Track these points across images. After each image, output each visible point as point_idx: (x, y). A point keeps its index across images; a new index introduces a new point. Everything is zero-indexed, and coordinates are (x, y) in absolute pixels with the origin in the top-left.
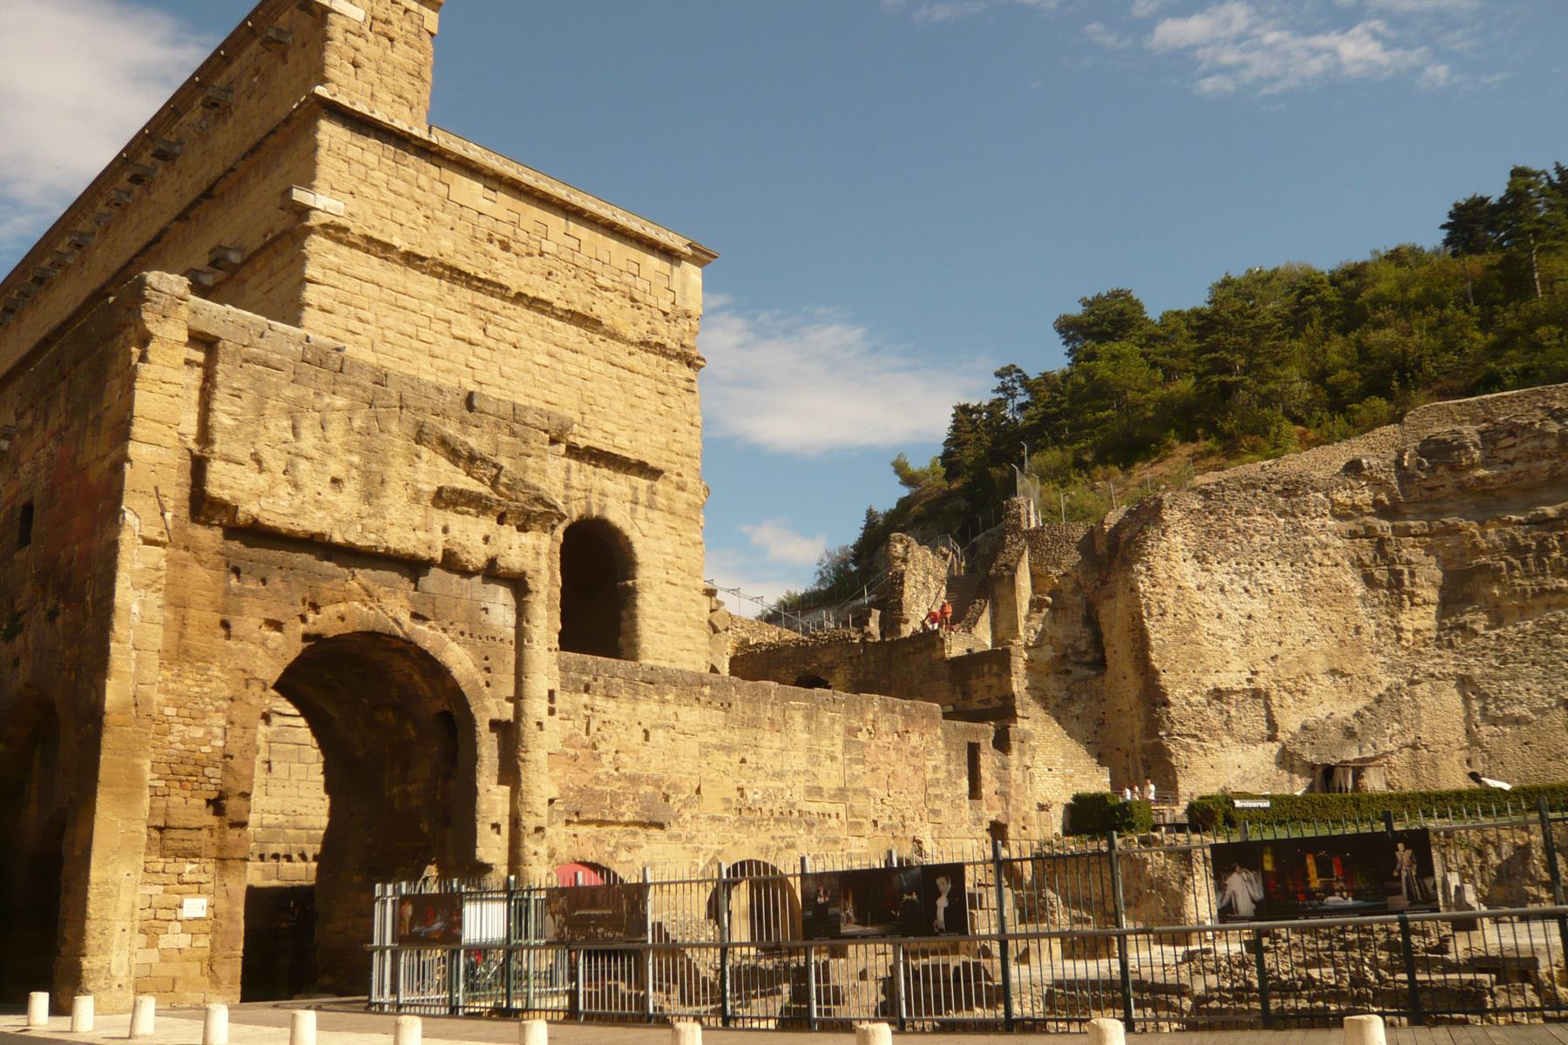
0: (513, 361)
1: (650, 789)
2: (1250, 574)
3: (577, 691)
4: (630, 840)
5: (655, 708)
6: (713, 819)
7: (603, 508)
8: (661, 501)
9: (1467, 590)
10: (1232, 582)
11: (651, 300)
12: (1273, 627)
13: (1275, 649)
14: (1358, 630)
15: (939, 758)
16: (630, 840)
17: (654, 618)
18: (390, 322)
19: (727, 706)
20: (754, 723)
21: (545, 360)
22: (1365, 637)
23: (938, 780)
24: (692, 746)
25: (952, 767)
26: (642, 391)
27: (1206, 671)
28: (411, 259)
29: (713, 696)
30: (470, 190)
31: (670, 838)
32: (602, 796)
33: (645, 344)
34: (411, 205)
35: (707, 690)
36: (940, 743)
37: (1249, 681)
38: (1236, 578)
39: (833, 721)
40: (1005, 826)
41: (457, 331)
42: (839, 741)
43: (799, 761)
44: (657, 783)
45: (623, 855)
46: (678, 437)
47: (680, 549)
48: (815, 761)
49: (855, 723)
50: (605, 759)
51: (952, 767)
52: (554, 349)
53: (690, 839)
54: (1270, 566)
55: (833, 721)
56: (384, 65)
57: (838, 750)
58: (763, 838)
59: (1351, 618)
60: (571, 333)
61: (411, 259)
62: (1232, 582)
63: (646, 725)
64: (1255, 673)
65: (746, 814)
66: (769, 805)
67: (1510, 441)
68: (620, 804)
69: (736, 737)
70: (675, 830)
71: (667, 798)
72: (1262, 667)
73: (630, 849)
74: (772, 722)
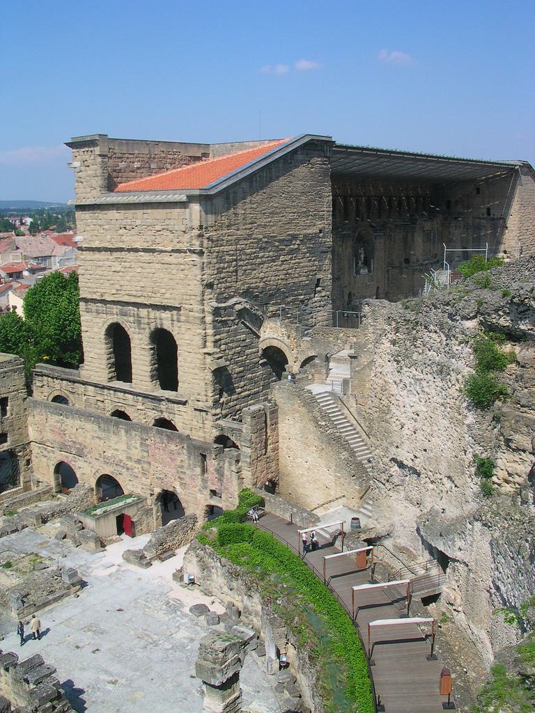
1: (79, 446)
6: (96, 459)
7: (162, 324)
8: (183, 318)
11: (176, 229)
15: (184, 457)
20: (108, 431)
21: (139, 270)
24: (89, 435)
28: (99, 250)
30: (113, 214)
33: (173, 251)
34: (98, 227)
36: (185, 451)
39: (136, 435)
42: (138, 442)
43: (124, 447)
44: (80, 444)
45: (73, 463)
48: (129, 448)
50: (67, 435)
52: (142, 264)
53: (90, 463)
55: (136, 435)
57: (138, 446)
58: (112, 469)
60: (146, 257)
61: (99, 250)
69: (102, 435)
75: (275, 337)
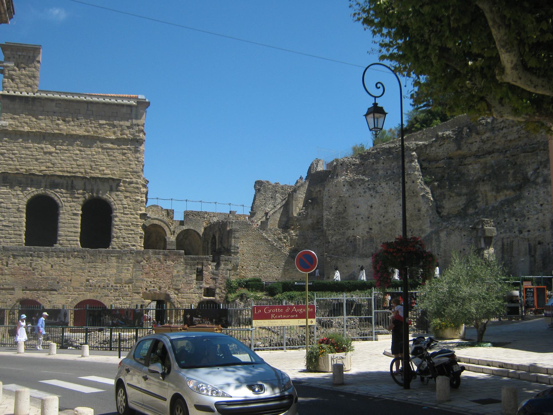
0: (65, 155)
2: (374, 189)
3: (28, 256)
4: (44, 294)
5: (56, 259)
9: (477, 189)
10: (365, 192)
12: (382, 210)
13: (381, 219)
14: (419, 210)
16: (44, 294)
17: (117, 225)
18: (23, 152)
19: (83, 258)
21: (78, 152)
22: (422, 213)
23: (179, 275)
25: (187, 271)
26: (116, 154)
27: (349, 229)
29: (78, 255)
31: (58, 293)
32: (35, 283)
35: (76, 253)
37: (368, 232)
38: (367, 190)
40: (215, 289)
41: (45, 150)
44: (55, 279)
46: (132, 166)
47: (130, 203)
49: (140, 259)
51: (187, 271)
54: (383, 184)
56: (22, 77)
59: (417, 205)
62: (365, 192)
63: (52, 263)
64: (371, 229)
65: (90, 287)
66: (99, 284)
68: (41, 285)
70: (60, 291)
71: (58, 283)
72: (374, 227)
73: (43, 297)
74: (102, 260)
75: (156, 217)
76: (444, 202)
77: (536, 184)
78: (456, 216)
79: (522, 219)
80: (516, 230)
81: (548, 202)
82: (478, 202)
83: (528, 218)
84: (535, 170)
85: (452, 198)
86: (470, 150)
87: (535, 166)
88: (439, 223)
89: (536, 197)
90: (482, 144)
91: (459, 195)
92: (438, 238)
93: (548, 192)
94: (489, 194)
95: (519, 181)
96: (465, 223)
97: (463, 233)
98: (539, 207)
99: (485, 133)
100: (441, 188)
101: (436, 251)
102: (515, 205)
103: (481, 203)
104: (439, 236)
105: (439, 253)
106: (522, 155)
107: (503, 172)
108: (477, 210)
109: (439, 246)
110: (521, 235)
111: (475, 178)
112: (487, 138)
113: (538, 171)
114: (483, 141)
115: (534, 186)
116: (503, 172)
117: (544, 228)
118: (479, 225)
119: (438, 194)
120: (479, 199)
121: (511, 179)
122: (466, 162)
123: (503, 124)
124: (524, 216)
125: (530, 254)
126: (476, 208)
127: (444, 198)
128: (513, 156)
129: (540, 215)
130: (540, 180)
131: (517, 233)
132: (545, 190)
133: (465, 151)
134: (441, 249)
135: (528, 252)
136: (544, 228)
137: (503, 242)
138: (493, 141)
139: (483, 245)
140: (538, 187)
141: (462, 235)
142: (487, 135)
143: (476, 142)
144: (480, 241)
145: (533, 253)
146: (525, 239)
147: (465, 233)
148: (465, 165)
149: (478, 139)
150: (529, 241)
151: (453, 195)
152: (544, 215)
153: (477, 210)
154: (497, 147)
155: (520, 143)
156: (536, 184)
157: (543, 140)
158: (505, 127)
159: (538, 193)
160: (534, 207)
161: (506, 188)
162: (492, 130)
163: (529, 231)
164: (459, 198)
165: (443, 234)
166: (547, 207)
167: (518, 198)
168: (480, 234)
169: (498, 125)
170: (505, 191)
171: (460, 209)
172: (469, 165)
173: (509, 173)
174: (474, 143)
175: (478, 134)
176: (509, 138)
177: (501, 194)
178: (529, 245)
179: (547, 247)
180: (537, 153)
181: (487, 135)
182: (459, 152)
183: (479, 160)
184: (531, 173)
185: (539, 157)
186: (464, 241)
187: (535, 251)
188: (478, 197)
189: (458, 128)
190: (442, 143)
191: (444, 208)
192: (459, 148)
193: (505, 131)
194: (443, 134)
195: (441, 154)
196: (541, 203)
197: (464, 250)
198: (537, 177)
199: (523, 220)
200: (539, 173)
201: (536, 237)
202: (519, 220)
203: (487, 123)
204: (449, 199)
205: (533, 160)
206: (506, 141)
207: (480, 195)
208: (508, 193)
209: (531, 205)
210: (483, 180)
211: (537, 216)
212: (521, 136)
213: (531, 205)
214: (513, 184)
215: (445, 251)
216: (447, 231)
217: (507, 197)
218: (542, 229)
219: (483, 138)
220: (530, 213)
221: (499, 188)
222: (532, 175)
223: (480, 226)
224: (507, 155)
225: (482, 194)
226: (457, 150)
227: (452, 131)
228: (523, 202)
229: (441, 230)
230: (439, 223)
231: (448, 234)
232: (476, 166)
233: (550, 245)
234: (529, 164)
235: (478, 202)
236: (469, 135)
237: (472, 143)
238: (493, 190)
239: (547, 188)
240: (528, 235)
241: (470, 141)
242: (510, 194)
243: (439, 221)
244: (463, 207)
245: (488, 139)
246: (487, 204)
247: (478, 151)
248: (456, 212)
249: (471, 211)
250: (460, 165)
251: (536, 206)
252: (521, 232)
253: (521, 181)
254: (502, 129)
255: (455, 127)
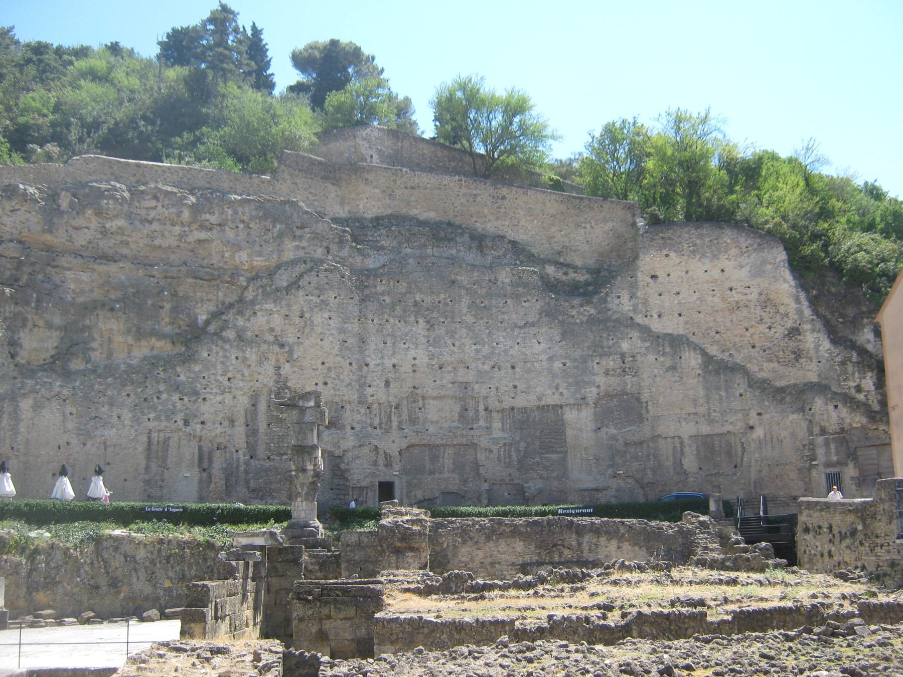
9: (87, 322)
67: (153, 203)
76: (22, 335)
77: (225, 340)
78: (42, 367)
79: (193, 399)
80: (179, 417)
81: (243, 375)
82: (93, 350)
83: (204, 399)
84: (215, 315)
85: (36, 329)
86: (70, 240)
87: (212, 307)
88: (15, 378)
89: (222, 363)
90: (100, 236)
91: (50, 326)
92: (16, 412)
93: (245, 359)
94: (119, 339)
95: (179, 327)
96: (74, 388)
97: (69, 409)
98: (226, 383)
99: (116, 217)
100: (16, 304)
101: (7, 441)
102: (179, 369)
103: (97, 353)
104: (16, 409)
105: (15, 446)
106: (190, 280)
107: (150, 302)
108: (89, 366)
109: (15, 430)
110: (188, 429)
111: (81, 299)
112: (119, 228)
113: (224, 317)
114: (104, 232)
115: (220, 343)
116: (150, 302)
117: (232, 422)
118: (308, 400)
119: (7, 315)
120: (95, 345)
121: (167, 320)
122: (63, 261)
123: (153, 214)
124: (197, 393)
125: (199, 467)
126: (88, 361)
127: (24, 326)
128: (166, 277)
129: (228, 396)
130: (230, 334)
131: (181, 423)
132: (240, 355)
133: (58, 239)
134: (20, 438)
135: (196, 461)
136: (232, 422)
137: (149, 438)
138: (125, 238)
139: (316, 442)
140: (227, 347)
141: (67, 412)
142: (121, 222)
143: (88, 228)
144: (312, 430)
145: (205, 465)
146: (195, 436)
147: (74, 411)
148: (54, 267)
149: (94, 223)
150: (200, 441)
151: (41, 323)
152: (234, 398)
153: (89, 366)
154: (125, 251)
155: (172, 257)
156: (225, 340)
157: (220, 265)
158: (159, 220)
159: (225, 357)
160: (217, 381)
161: (154, 333)
162: (129, 217)
163: (203, 423)
164: (48, 334)
165: (26, 404)
166: (241, 384)
167: (188, 359)
168: (308, 417)
169: (143, 213)
170: (154, 340)
171: (48, 355)
172: (70, 269)
173: (162, 307)
174: (85, 230)
175: (99, 213)
176: (157, 242)
177: (143, 343)
178: (200, 448)
179: (235, 455)
180: (218, 286)
181: (121, 222)
182: (48, 237)
183: (95, 266)
184: (204, 317)
185: (220, 294)
186: (70, 425)
187: (210, 461)
188: (94, 340)
189: (49, 188)
190: (17, 207)
191: (21, 346)
192: (50, 228)
193: (156, 226)
194: (25, 190)
195: (7, 229)
196: (230, 375)
197: (68, 444)
198: (222, 329)
199: (195, 402)
200: (225, 320)
201: (216, 436)
202: (186, 399)
203: (123, 198)
204: (31, 330)
205: (210, 296)
206: (150, 246)
207: (96, 336)
208: (159, 344)
209: (213, 377)
210: (112, 309)
211: (221, 397)
212: (183, 245)
213: (213, 377)
214: (168, 329)
215: (27, 443)
216: (35, 399)
217: (155, 352)
218: (226, 423)
219: (108, 225)
220: (208, 390)
221: (142, 331)
222: (207, 323)
223: (312, 403)
224: (155, 273)
225: (101, 336)
226: (44, 231)
227: (37, 189)
228: (197, 368)
229: (24, 396)
230: (15, 378)
231: (37, 407)
232: (85, 277)
233: (241, 453)
234: (202, 301)
235: (93, 350)
236: (78, 209)
237: (76, 228)
238: (129, 331)
239: (243, 351)
240: (202, 430)
241: (75, 223)
242: (162, 347)
243: (15, 374)
244: (53, 353)
245: (121, 231)
246: (110, 355)
247: (88, 247)
248: (42, 362)
249: (76, 365)
250: (49, 265)
251: (221, 378)
252: (186, 423)
253: (183, 328)
254: (150, 222)
255: (40, 183)
